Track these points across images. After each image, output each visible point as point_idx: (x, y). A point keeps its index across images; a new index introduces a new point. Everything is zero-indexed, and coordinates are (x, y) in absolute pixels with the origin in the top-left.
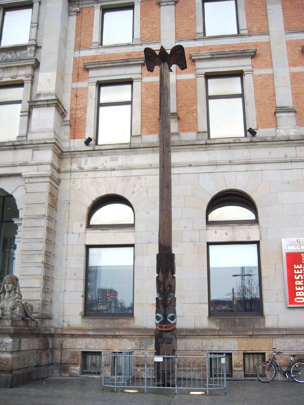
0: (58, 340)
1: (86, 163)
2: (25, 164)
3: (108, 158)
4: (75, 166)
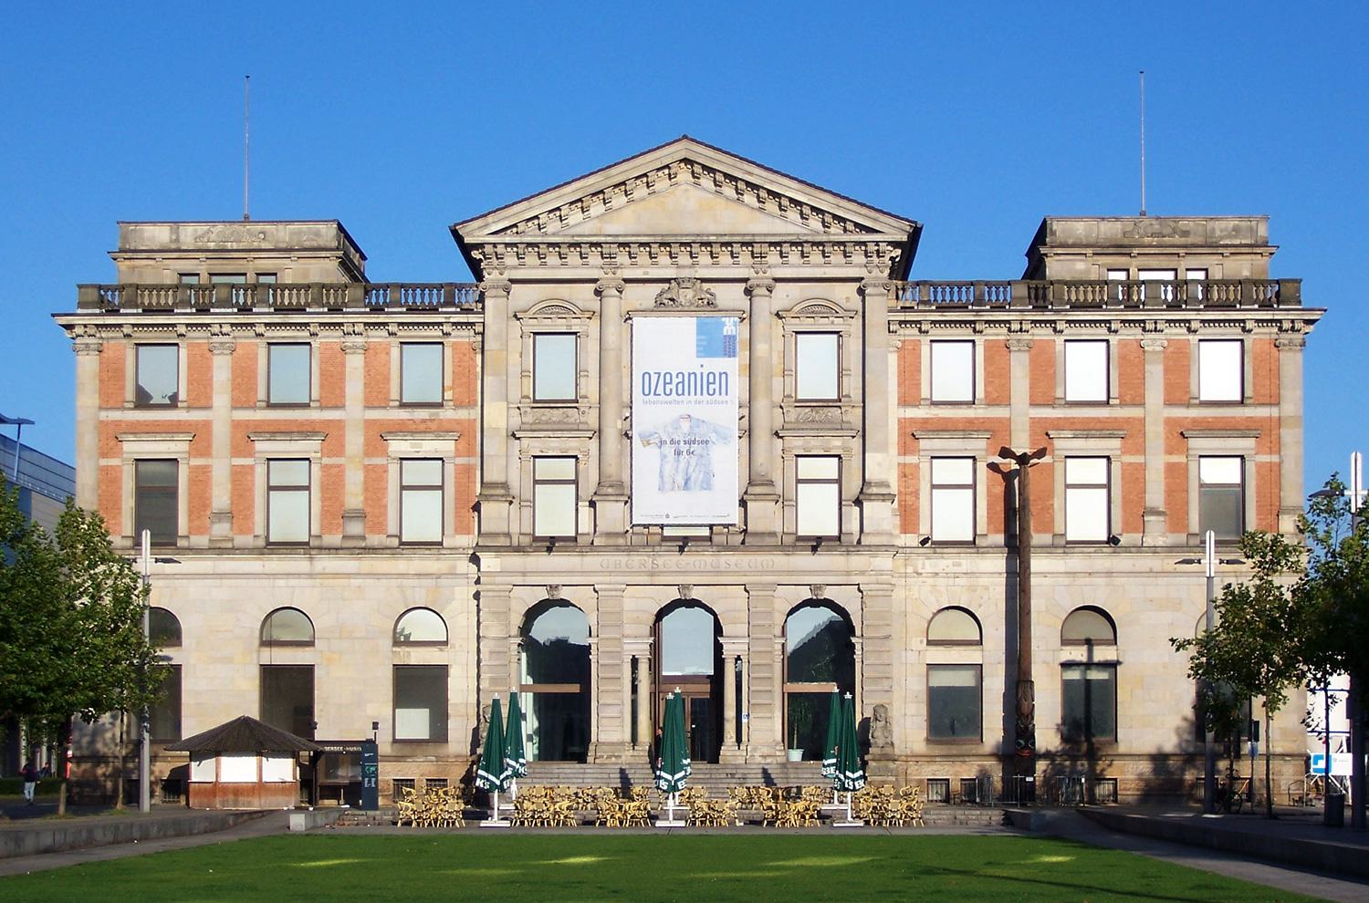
2: (862, 573)
4: (910, 570)
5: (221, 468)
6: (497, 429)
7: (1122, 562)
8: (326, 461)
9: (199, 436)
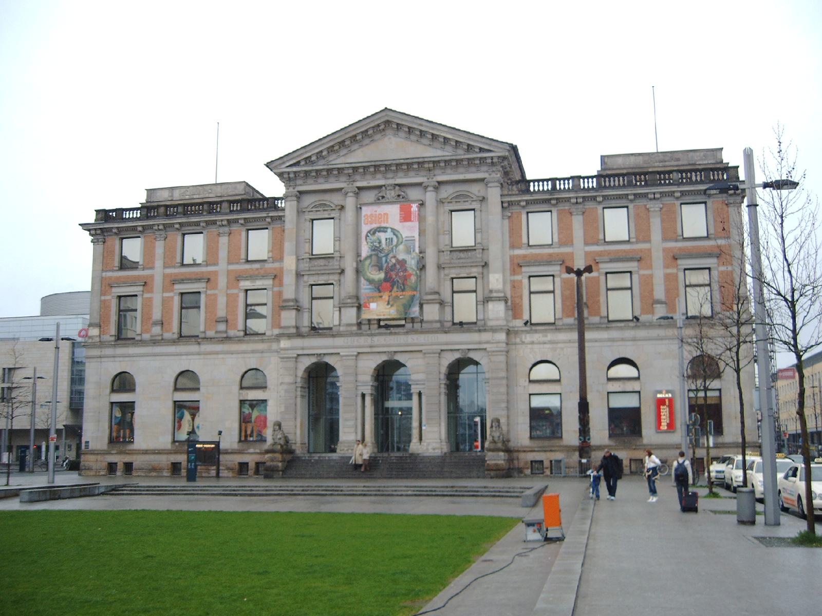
0: (515, 454)
1: (525, 338)
2: (488, 342)
3: (540, 335)
4: (518, 340)
5: (157, 297)
7: (642, 333)
9: (146, 284)
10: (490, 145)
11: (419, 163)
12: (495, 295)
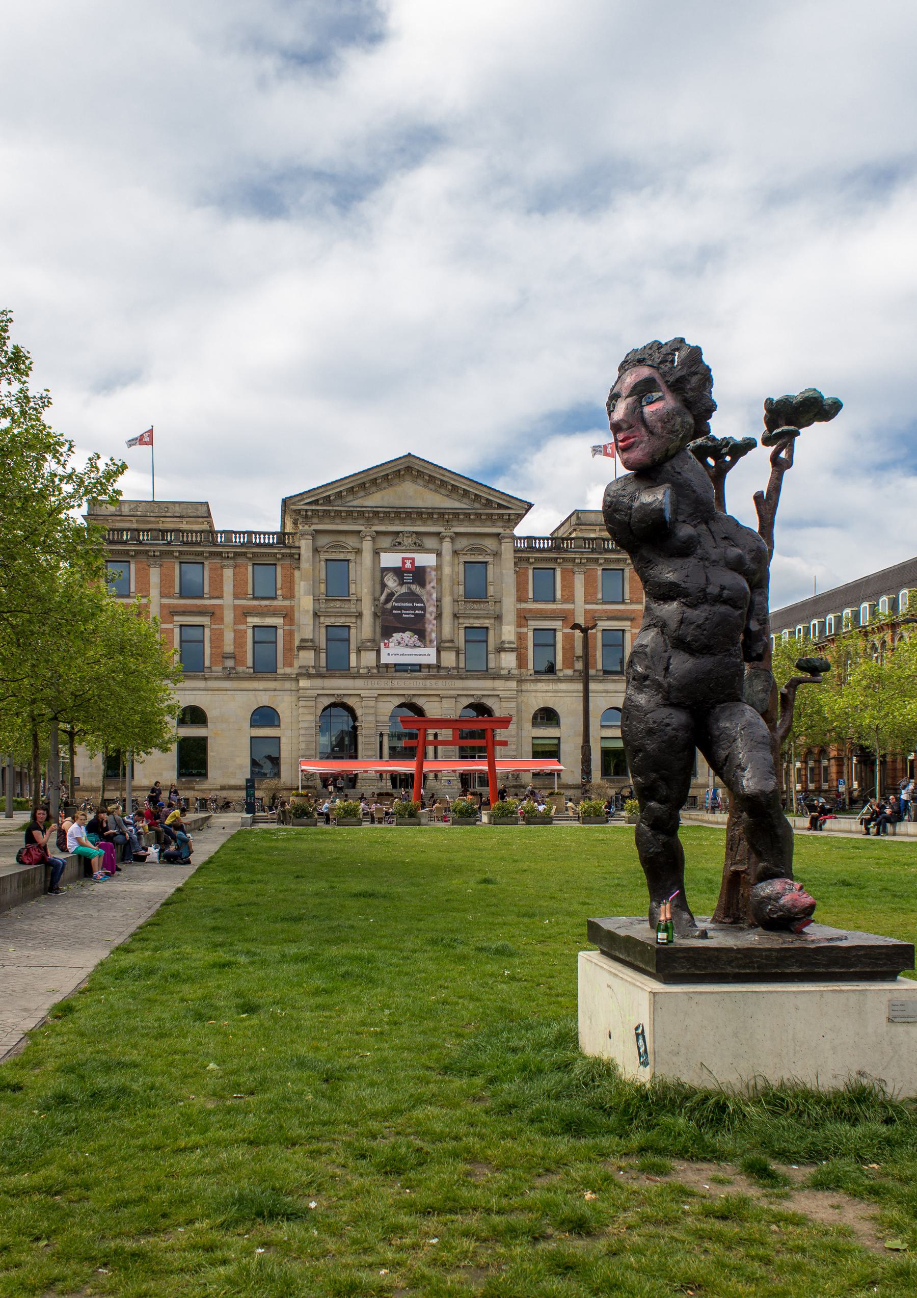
6: (307, 611)
8: (214, 626)
10: (509, 502)
11: (439, 513)
12: (507, 645)
